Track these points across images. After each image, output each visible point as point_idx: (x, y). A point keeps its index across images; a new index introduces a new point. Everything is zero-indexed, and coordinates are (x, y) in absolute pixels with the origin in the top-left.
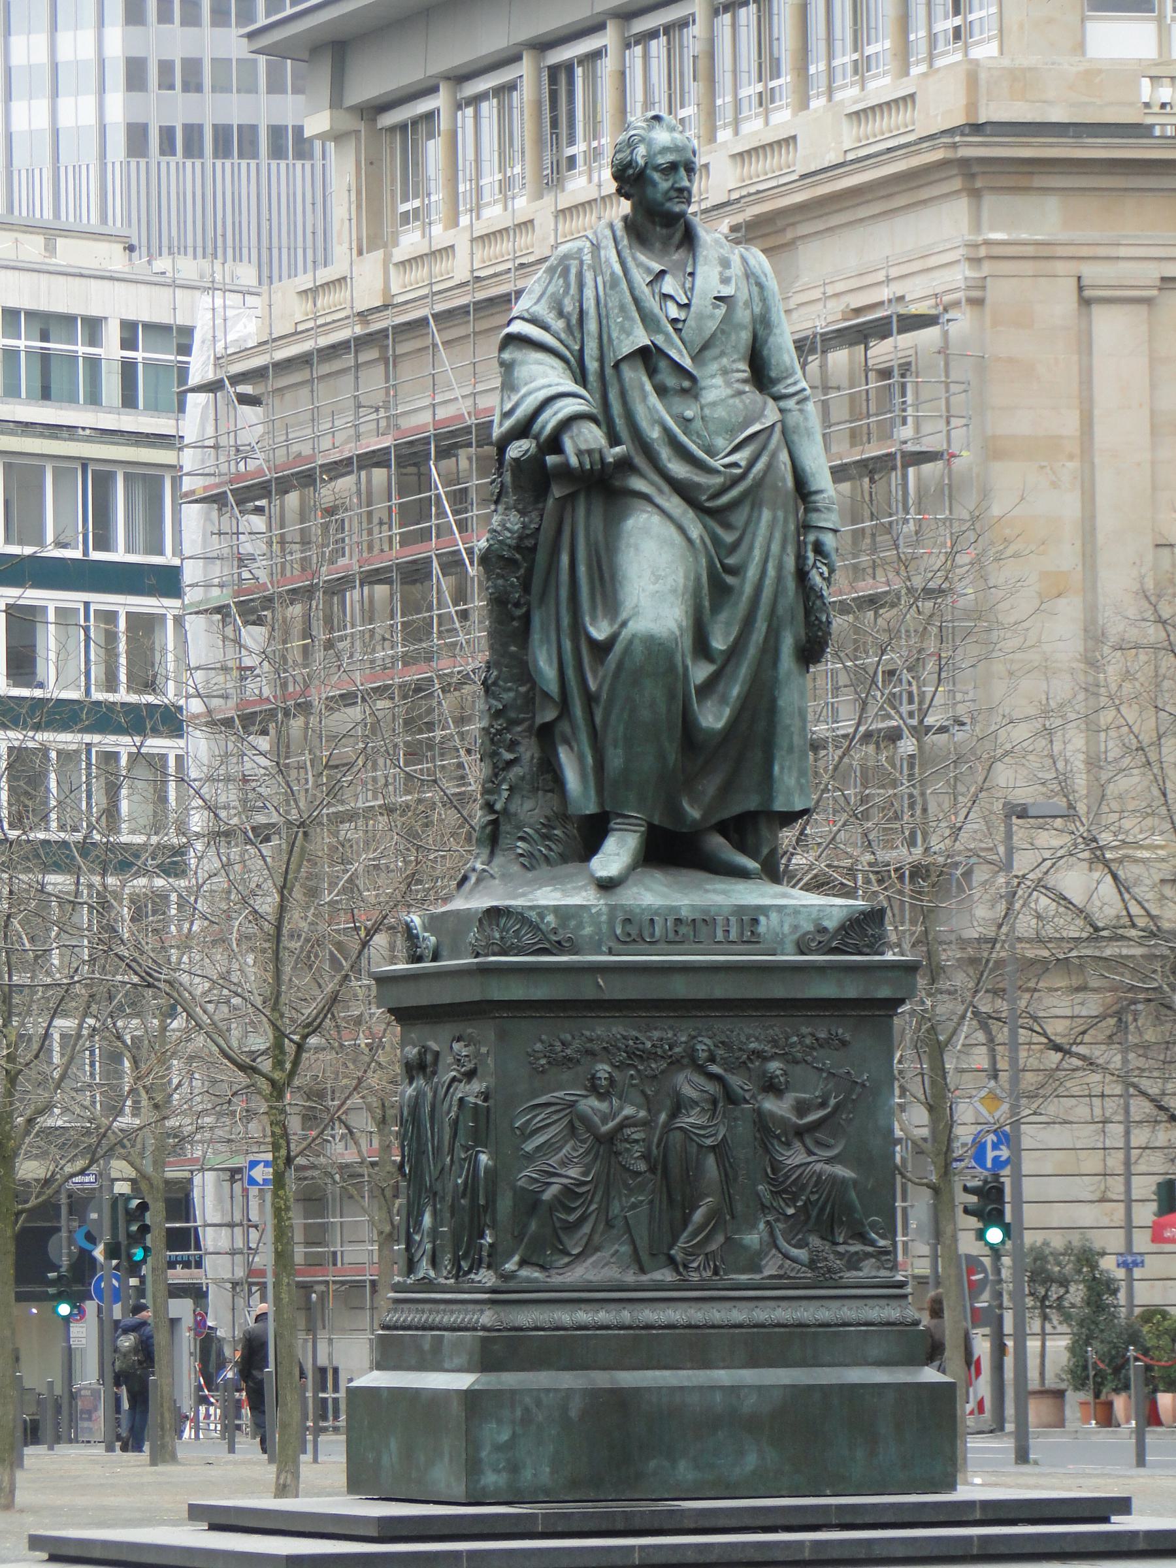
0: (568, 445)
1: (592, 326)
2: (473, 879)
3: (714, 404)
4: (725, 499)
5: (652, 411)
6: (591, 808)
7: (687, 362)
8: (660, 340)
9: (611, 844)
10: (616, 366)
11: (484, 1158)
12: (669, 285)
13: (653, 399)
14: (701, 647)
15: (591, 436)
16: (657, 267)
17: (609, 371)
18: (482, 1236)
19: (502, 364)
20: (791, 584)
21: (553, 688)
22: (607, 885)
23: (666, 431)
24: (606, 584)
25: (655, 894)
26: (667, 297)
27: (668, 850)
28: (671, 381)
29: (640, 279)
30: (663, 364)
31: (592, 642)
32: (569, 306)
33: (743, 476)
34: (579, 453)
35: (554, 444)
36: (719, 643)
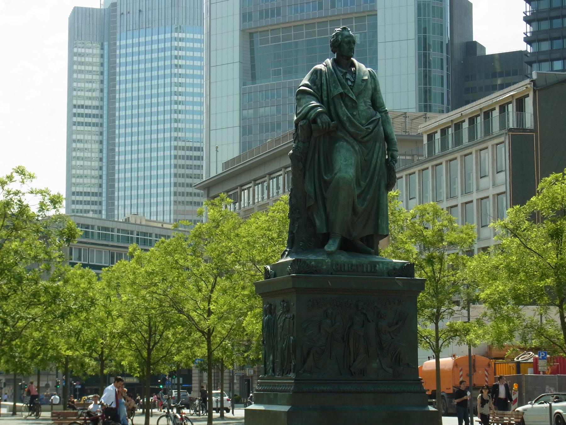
0: (319, 121)
1: (325, 87)
2: (287, 253)
3: (362, 111)
4: (366, 139)
5: (343, 111)
6: (325, 231)
7: (354, 98)
8: (346, 91)
9: (331, 242)
10: (333, 98)
11: (292, 338)
12: (348, 76)
13: (344, 108)
14: (358, 184)
15: (326, 118)
16: (344, 71)
17: (330, 100)
18: (291, 362)
19: (297, 99)
20: (384, 166)
21: (313, 194)
22: (329, 254)
23: (348, 117)
24: (329, 164)
25: (344, 258)
26: (347, 79)
27: (347, 246)
28: (349, 104)
29: (340, 75)
30: (347, 99)
31: (325, 181)
32: (318, 82)
33: (372, 132)
34: (322, 123)
35: (314, 121)
36: (363, 184)
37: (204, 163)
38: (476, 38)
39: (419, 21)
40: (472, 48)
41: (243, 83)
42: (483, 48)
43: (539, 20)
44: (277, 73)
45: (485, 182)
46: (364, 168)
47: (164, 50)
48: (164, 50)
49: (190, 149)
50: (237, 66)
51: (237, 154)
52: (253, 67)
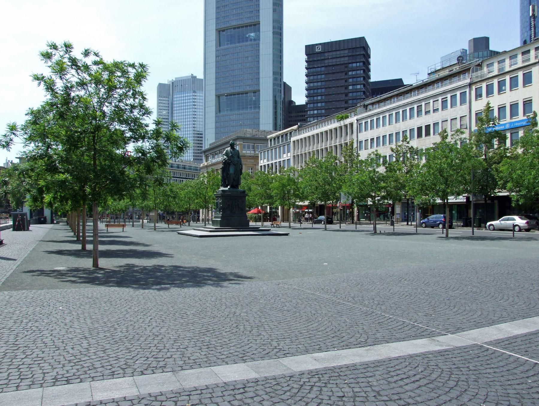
37: (203, 146)
38: (293, 99)
39: (274, 94)
40: (291, 102)
41: (216, 113)
42: (295, 103)
43: (310, 97)
44: (227, 110)
45: (285, 155)
46: (236, 170)
47: (190, 99)
48: (190, 99)
49: (198, 134)
50: (214, 107)
51: (214, 141)
52: (219, 107)
